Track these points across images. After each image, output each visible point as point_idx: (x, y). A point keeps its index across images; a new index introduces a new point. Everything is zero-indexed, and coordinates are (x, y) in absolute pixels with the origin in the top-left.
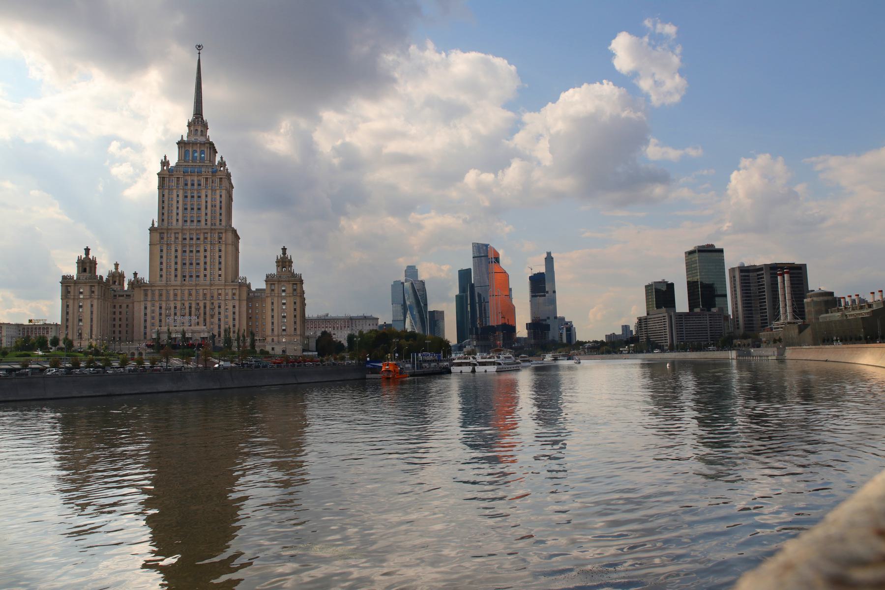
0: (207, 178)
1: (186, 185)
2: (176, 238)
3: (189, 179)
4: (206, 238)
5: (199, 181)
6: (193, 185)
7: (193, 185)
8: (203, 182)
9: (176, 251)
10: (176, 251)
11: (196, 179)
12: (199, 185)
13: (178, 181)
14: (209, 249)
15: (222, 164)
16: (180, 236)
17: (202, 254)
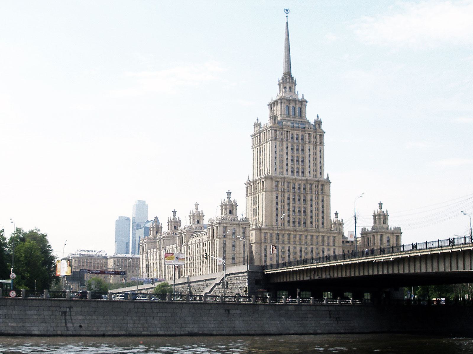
0: (310, 134)
1: (292, 138)
2: (288, 187)
3: (295, 133)
4: (311, 189)
5: (302, 135)
6: (297, 139)
7: (297, 139)
8: (306, 137)
9: (289, 198)
10: (289, 198)
11: (300, 133)
12: (302, 139)
13: (287, 134)
14: (314, 199)
15: (318, 123)
16: (292, 186)
17: (309, 203)
